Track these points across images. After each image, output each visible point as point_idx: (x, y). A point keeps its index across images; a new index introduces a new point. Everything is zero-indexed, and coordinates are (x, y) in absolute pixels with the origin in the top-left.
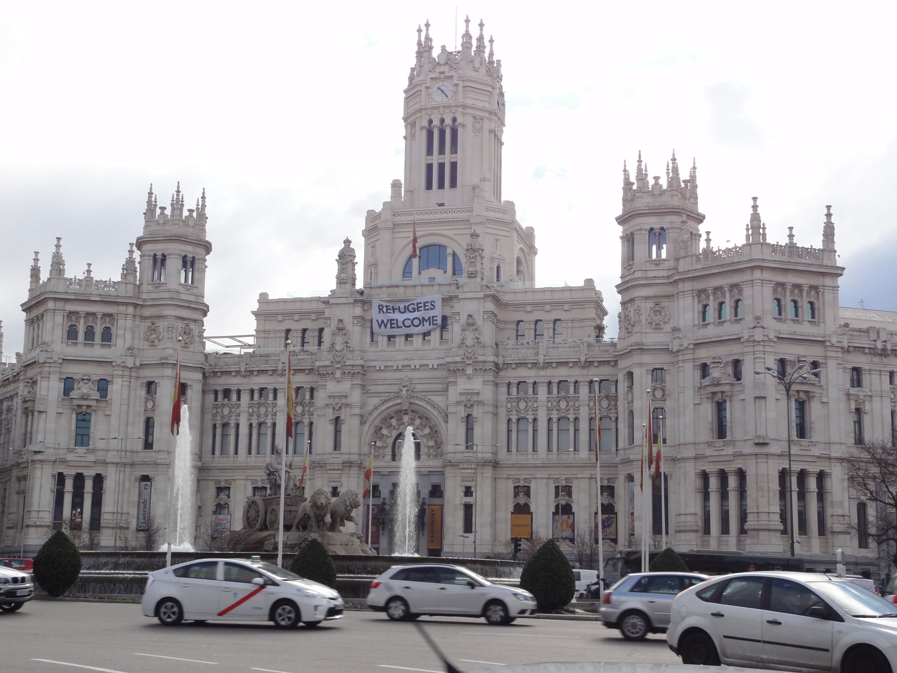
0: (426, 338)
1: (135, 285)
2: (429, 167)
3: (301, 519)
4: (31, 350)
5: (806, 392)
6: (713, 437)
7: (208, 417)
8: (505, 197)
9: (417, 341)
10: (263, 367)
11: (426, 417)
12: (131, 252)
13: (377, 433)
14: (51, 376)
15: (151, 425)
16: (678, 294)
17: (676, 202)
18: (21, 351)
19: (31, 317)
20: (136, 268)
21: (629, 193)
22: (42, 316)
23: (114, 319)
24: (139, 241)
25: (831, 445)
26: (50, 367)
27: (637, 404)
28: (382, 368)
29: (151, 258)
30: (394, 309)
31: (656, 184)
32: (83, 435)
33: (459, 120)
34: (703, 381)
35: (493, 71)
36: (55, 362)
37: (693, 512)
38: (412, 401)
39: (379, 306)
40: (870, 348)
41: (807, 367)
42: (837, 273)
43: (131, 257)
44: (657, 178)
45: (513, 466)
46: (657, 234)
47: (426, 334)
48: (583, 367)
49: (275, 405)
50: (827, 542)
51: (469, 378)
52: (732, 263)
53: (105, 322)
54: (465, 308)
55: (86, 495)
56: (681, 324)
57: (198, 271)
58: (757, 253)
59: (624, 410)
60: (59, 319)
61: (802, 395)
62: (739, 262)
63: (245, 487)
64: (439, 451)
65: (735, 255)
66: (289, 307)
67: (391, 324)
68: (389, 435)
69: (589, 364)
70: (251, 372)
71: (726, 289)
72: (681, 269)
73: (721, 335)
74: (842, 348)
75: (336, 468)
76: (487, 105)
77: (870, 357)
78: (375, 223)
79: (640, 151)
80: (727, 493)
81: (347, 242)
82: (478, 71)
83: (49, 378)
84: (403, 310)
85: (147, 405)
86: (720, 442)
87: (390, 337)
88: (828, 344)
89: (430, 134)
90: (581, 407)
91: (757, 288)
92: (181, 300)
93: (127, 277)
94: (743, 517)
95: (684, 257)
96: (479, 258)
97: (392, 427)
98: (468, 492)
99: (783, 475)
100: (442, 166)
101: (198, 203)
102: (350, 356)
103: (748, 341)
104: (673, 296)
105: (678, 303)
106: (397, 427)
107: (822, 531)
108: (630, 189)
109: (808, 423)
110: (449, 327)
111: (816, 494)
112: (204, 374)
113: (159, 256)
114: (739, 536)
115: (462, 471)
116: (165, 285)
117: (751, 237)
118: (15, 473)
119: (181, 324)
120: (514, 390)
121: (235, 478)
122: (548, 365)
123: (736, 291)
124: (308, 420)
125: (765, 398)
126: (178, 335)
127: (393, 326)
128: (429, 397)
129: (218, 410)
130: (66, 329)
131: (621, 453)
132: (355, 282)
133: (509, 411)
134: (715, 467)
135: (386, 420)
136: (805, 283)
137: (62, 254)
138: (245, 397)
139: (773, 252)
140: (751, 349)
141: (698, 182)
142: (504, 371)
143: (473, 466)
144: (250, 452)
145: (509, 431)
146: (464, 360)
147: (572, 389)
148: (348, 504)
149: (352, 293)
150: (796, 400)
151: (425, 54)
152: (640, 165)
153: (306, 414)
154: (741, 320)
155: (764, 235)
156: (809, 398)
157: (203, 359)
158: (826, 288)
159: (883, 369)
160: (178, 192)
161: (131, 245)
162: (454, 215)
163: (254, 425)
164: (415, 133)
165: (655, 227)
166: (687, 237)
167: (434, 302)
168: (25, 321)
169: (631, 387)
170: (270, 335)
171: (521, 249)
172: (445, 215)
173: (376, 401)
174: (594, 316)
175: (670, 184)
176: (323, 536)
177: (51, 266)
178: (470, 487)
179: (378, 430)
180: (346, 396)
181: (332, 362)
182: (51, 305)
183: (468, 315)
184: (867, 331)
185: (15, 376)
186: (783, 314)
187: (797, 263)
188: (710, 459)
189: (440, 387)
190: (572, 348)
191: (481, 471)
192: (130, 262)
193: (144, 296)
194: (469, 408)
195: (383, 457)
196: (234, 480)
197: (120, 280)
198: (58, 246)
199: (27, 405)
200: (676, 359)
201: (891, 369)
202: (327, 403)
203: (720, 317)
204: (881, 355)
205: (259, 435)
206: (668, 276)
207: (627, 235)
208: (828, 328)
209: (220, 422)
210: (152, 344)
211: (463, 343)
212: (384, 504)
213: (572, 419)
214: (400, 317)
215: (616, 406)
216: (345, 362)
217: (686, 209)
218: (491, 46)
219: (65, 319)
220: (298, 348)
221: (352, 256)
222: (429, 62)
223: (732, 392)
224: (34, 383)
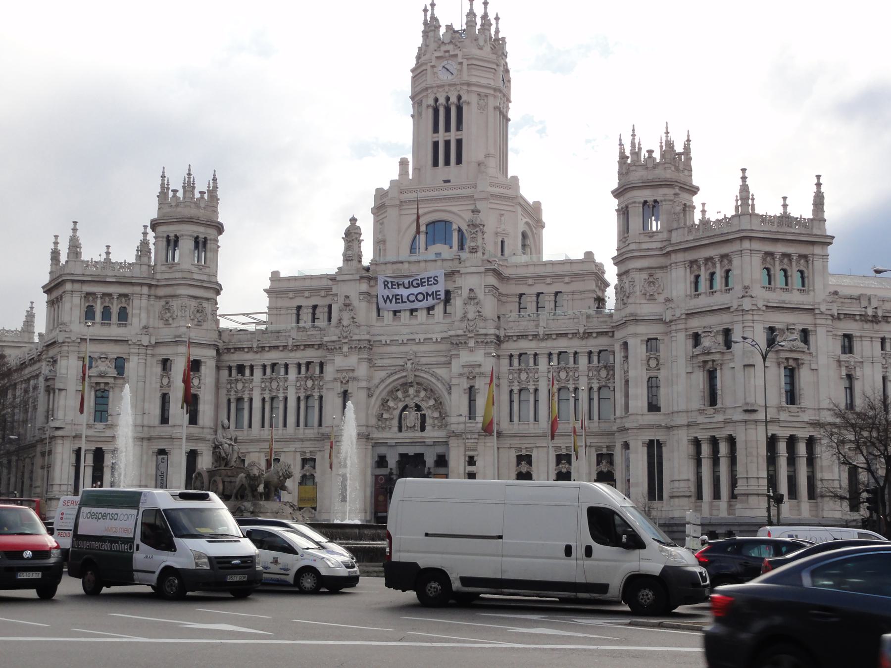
0: (431, 312)
1: (149, 266)
2: (436, 145)
3: (240, 489)
4: (52, 330)
5: (796, 360)
6: (704, 405)
7: (223, 392)
8: (510, 174)
9: (422, 315)
10: (274, 343)
11: (431, 390)
12: (145, 234)
14: (71, 356)
15: (167, 400)
16: (671, 265)
17: (669, 174)
18: (43, 331)
19: (52, 299)
20: (150, 249)
21: (624, 167)
22: (61, 296)
23: (129, 299)
24: (153, 223)
25: (821, 411)
26: (69, 346)
27: (632, 374)
28: (388, 342)
29: (165, 239)
30: (399, 285)
31: (650, 157)
32: (102, 411)
33: (463, 99)
34: (694, 350)
35: (498, 46)
36: (74, 342)
37: (687, 478)
38: (417, 373)
39: (384, 282)
40: (861, 315)
41: (796, 335)
42: (826, 241)
43: (145, 239)
44: (650, 152)
45: (515, 436)
46: (651, 206)
47: (430, 309)
48: (582, 339)
49: (286, 380)
50: (817, 506)
51: (346, 356)
52: (722, 234)
53: (122, 303)
54: (466, 283)
55: (105, 469)
56: (674, 294)
57: (211, 251)
58: (745, 224)
59: (621, 380)
60: (77, 300)
61: (791, 362)
62: (728, 233)
64: (443, 421)
65: (725, 226)
66: (299, 284)
67: (396, 299)
69: (587, 335)
70: (263, 348)
71: (717, 260)
72: (674, 241)
73: (712, 305)
74: (832, 316)
76: (492, 83)
77: (860, 323)
78: (383, 200)
79: (634, 126)
80: (718, 459)
81: (353, 220)
82: (481, 48)
83: (68, 357)
84: (407, 286)
85: (163, 381)
86: (711, 410)
87: (395, 312)
88: (817, 311)
89: (436, 112)
90: (580, 377)
91: (746, 258)
92: (194, 279)
93: (142, 258)
94: (733, 483)
95: (676, 229)
96: (480, 234)
97: (398, 399)
98: (471, 461)
99: (772, 442)
100: (447, 143)
101: (209, 185)
102: (357, 331)
103: (737, 310)
104: (667, 267)
105: (671, 274)
106: (403, 399)
107: (812, 495)
108: (625, 163)
109: (798, 387)
110: (452, 301)
111: (805, 459)
112: (218, 351)
113: (172, 238)
114: (729, 501)
116: (178, 266)
117: (740, 207)
118: (39, 448)
119: (193, 303)
120: (516, 362)
122: (548, 336)
123: (726, 261)
124: (318, 394)
125: (754, 366)
126: (191, 313)
127: (398, 301)
128: (434, 370)
129: (233, 385)
130: (84, 309)
131: (617, 421)
132: (361, 259)
133: (511, 382)
134: (706, 434)
135: (392, 392)
136: (794, 252)
137: (78, 237)
138: (258, 373)
139: (762, 222)
140: (740, 318)
141: (692, 155)
142: (505, 343)
143: (476, 436)
144: (263, 426)
145: (511, 402)
146: (466, 333)
147: (571, 360)
148: (281, 474)
149: (358, 270)
150: (785, 368)
151: (431, 34)
152: (633, 139)
153: (316, 388)
154: (731, 289)
155: (753, 205)
156: (798, 365)
157: (215, 335)
158: (815, 257)
159: (874, 335)
160: (189, 174)
161: (145, 227)
162: (459, 191)
163: (267, 399)
164: (421, 112)
165: (648, 199)
166: (679, 209)
167: (437, 277)
168: (47, 302)
169: (626, 357)
170: (282, 312)
171: (527, 223)
172: (450, 192)
173: (383, 374)
174: (594, 287)
175: (663, 156)
176: (255, 505)
177: (69, 249)
178: (473, 457)
179: (385, 402)
180: (353, 370)
181: (339, 338)
182: (68, 286)
183: (471, 290)
184: (858, 298)
185: (39, 355)
186: (773, 283)
187: (786, 233)
188: (701, 426)
189: (443, 359)
190: (572, 320)
192: (144, 243)
193: (158, 276)
194: (471, 379)
195: (390, 428)
197: (134, 261)
198: (75, 230)
199: (49, 383)
200: (669, 329)
201: (882, 336)
202: (336, 376)
203: (711, 287)
204: (872, 321)
206: (661, 248)
207: (622, 208)
208: (818, 295)
209: (234, 397)
210: (166, 322)
211: (465, 317)
212: (391, 474)
213: (571, 389)
214: (404, 292)
215: (614, 375)
216: (351, 337)
217: (679, 181)
218: (497, 24)
219: (83, 300)
220: (310, 324)
221: (357, 233)
222: (435, 41)
223: (722, 360)
224: (55, 362)
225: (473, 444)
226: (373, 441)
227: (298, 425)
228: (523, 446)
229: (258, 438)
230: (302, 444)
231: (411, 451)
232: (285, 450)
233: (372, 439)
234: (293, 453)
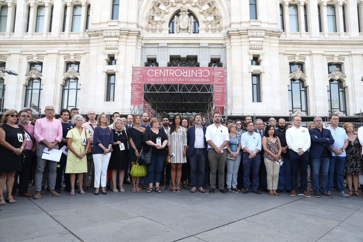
13: (154, 10)
63: (20, 61)
64: (218, 26)
68: (167, 11)
75: (113, 34)
97: (170, 4)
98: (256, 60)
106: (174, 4)
115: (250, 39)
121: (10, 52)
178: (259, 55)
191: (269, 40)
195: (161, 30)
196: (10, 54)
205: (38, 16)
225: (258, 43)
226: (144, 42)
227: (64, 30)
228: (298, 54)
229: (19, 39)
230: (66, 47)
231: (184, 53)
232: (48, 52)
233: (142, 39)
234: (56, 55)
